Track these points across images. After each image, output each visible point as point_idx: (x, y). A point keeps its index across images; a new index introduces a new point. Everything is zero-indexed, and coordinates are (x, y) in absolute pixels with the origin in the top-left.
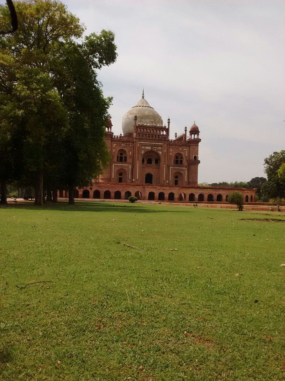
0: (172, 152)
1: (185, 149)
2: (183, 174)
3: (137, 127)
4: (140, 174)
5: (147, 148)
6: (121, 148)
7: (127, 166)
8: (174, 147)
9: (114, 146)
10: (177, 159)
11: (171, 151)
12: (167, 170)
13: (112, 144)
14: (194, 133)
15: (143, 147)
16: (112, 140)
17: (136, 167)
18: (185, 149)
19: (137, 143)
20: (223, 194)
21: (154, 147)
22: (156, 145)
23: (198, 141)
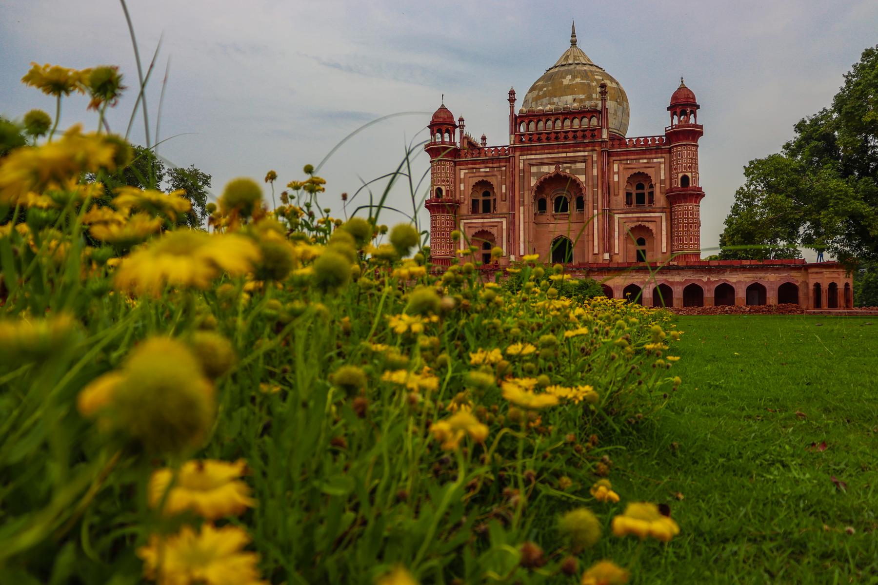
0: (618, 173)
1: (659, 160)
2: (654, 231)
3: (516, 117)
4: (529, 242)
5: (545, 169)
6: (481, 179)
7: (497, 223)
8: (625, 158)
9: (462, 176)
10: (639, 191)
11: (616, 170)
12: (603, 225)
13: (457, 172)
14: (678, 111)
15: (534, 169)
16: (455, 162)
17: (517, 223)
18: (659, 160)
19: (517, 161)
20: (735, 283)
21: (565, 165)
22: (568, 159)
23: (695, 133)
